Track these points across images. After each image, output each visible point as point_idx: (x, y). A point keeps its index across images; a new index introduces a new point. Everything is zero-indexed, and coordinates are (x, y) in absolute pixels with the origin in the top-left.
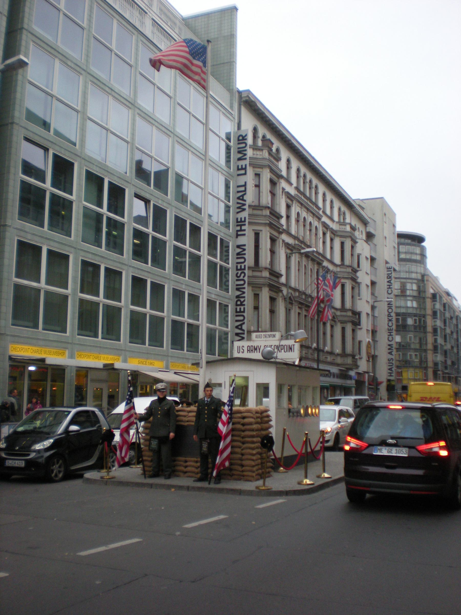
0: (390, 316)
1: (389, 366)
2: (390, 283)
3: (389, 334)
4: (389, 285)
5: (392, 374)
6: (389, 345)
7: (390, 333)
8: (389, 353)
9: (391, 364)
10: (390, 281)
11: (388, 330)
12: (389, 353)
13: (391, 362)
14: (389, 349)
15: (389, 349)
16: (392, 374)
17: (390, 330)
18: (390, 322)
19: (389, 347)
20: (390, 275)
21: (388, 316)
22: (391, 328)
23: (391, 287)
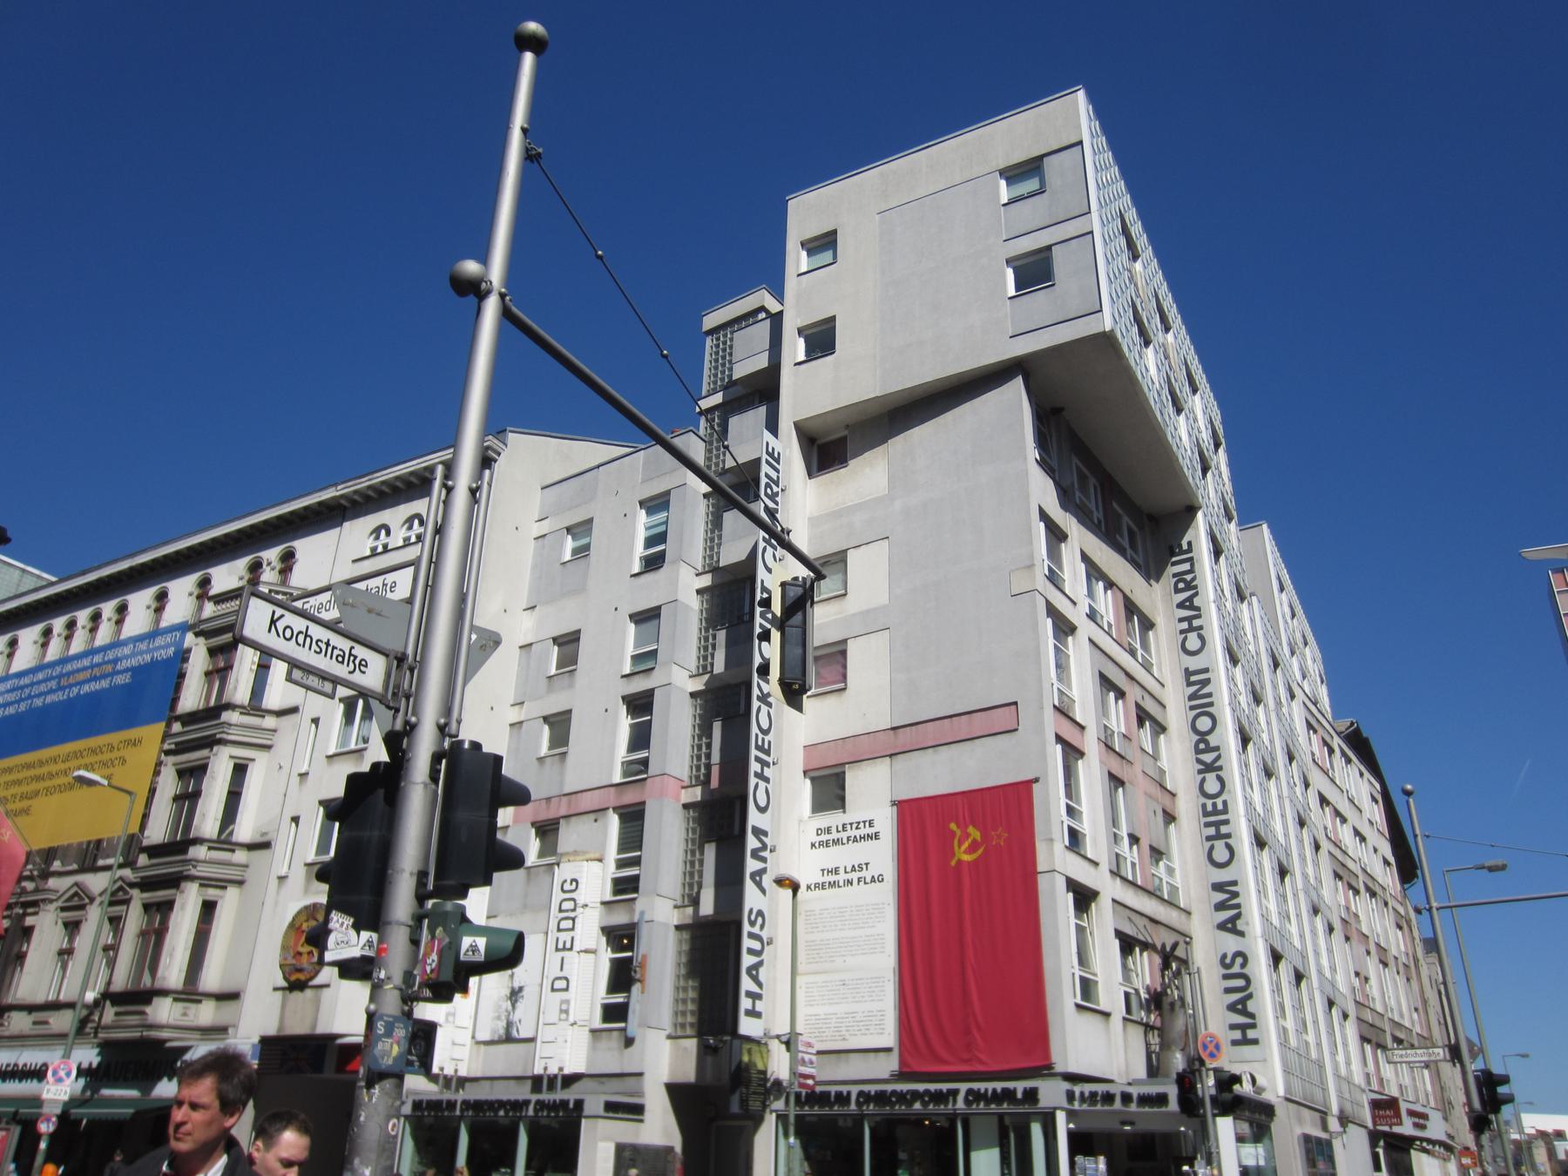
0: (1209, 749)
1: (1228, 991)
2: (1192, 607)
3: (1212, 831)
4: (1189, 619)
5: (1251, 1034)
6: (1218, 887)
7: (1217, 824)
8: (1222, 926)
9: (1240, 983)
10: (1190, 599)
11: (1206, 814)
12: (1222, 926)
13: (1236, 969)
14: (1220, 907)
15: (1220, 907)
16: (1251, 1034)
17: (1215, 812)
18: (1211, 778)
19: (1221, 897)
20: (1188, 577)
21: (1198, 751)
22: (1219, 801)
23: (1196, 623)
